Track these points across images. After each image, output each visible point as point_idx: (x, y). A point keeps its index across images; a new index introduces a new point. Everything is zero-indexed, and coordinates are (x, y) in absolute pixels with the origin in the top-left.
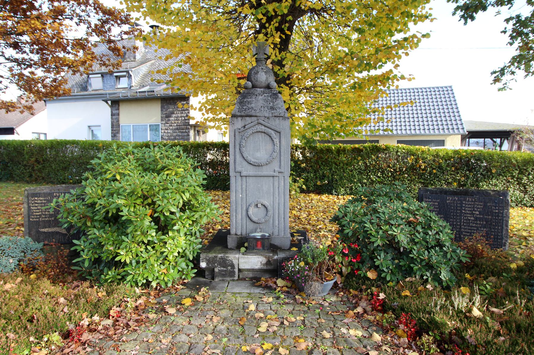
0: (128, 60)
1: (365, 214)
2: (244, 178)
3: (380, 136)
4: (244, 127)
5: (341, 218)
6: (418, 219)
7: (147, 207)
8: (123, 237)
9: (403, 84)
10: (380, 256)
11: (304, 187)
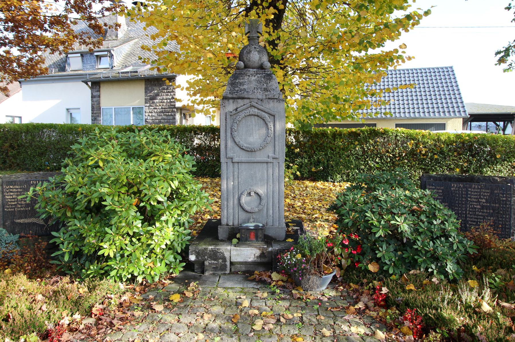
0: (110, 38)
1: (365, 203)
2: (236, 165)
3: (377, 119)
4: (236, 110)
5: (340, 207)
6: (421, 208)
7: (132, 196)
8: (106, 228)
10: (382, 248)
11: (298, 173)
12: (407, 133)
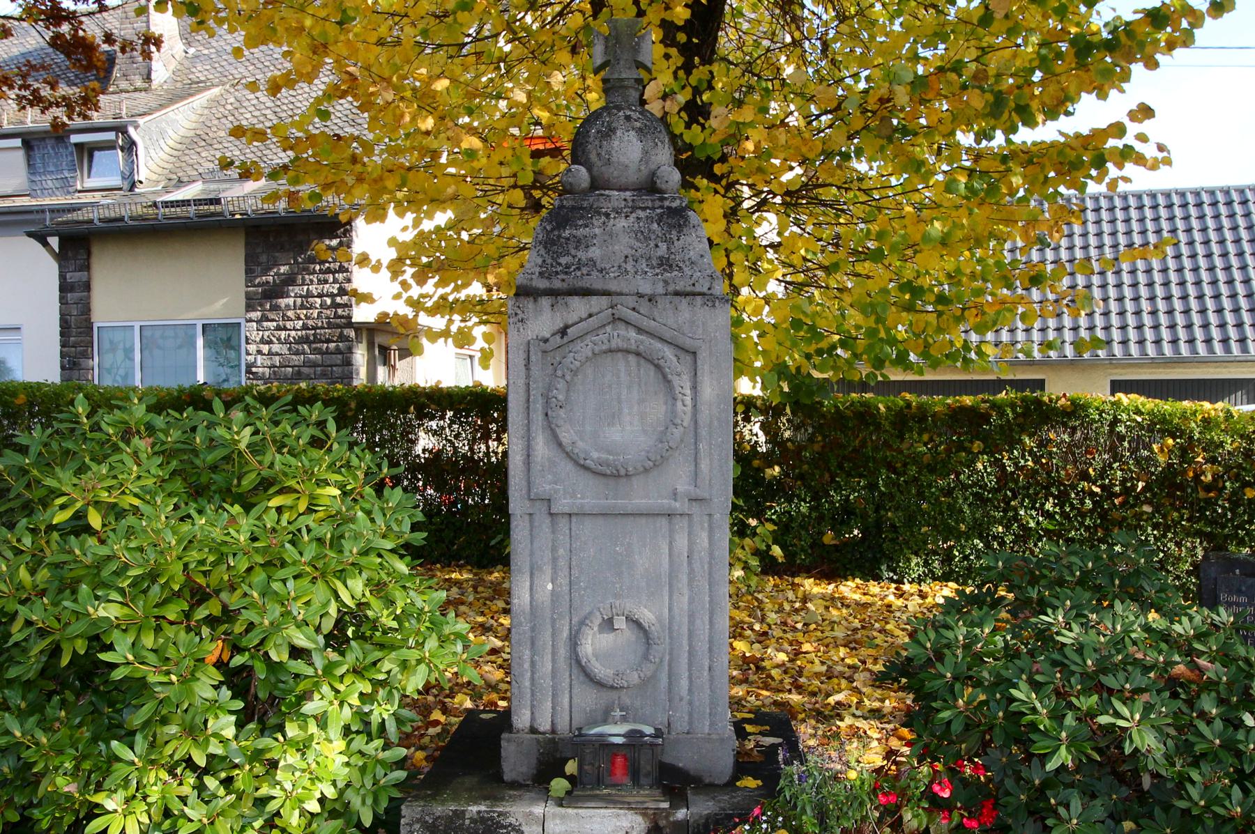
0: (124, 85)
1: (1010, 654)
2: (563, 523)
3: (1045, 363)
4: (563, 332)
5: (922, 667)
6: (1201, 671)
7: (205, 631)
8: (114, 743)
9: (1139, 179)
10: (1067, 807)
11: (777, 551)
12: (1151, 413)
